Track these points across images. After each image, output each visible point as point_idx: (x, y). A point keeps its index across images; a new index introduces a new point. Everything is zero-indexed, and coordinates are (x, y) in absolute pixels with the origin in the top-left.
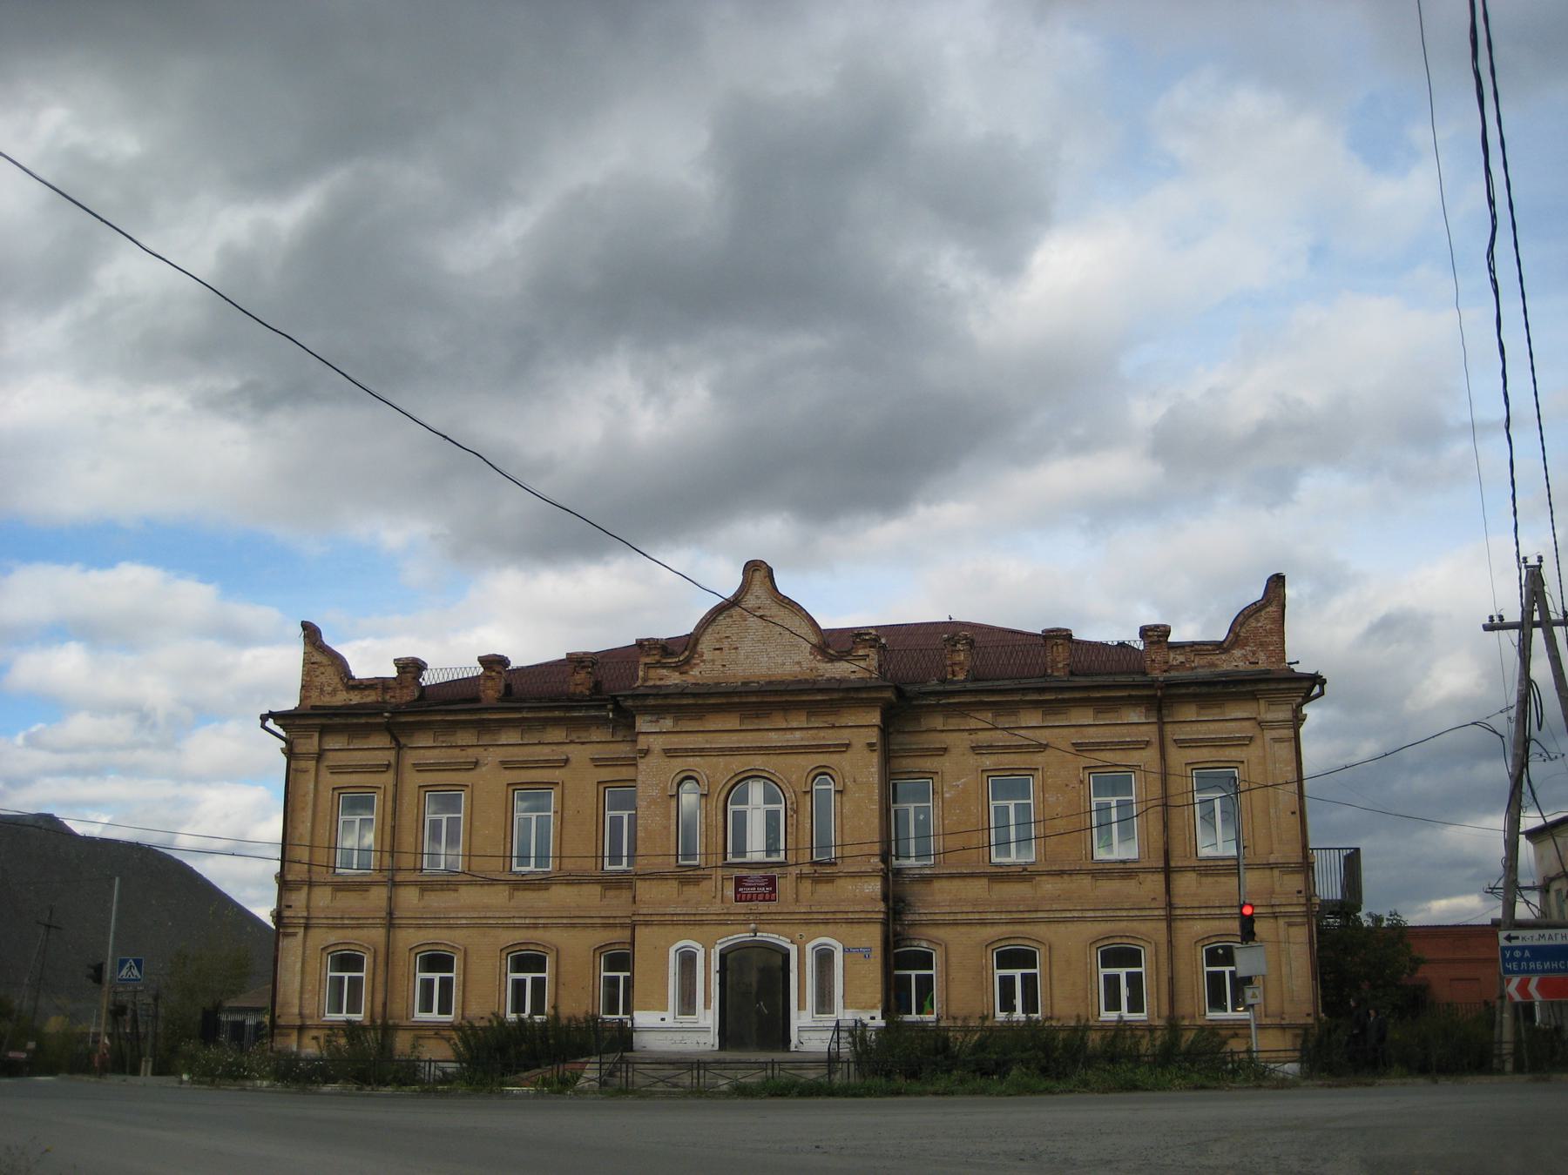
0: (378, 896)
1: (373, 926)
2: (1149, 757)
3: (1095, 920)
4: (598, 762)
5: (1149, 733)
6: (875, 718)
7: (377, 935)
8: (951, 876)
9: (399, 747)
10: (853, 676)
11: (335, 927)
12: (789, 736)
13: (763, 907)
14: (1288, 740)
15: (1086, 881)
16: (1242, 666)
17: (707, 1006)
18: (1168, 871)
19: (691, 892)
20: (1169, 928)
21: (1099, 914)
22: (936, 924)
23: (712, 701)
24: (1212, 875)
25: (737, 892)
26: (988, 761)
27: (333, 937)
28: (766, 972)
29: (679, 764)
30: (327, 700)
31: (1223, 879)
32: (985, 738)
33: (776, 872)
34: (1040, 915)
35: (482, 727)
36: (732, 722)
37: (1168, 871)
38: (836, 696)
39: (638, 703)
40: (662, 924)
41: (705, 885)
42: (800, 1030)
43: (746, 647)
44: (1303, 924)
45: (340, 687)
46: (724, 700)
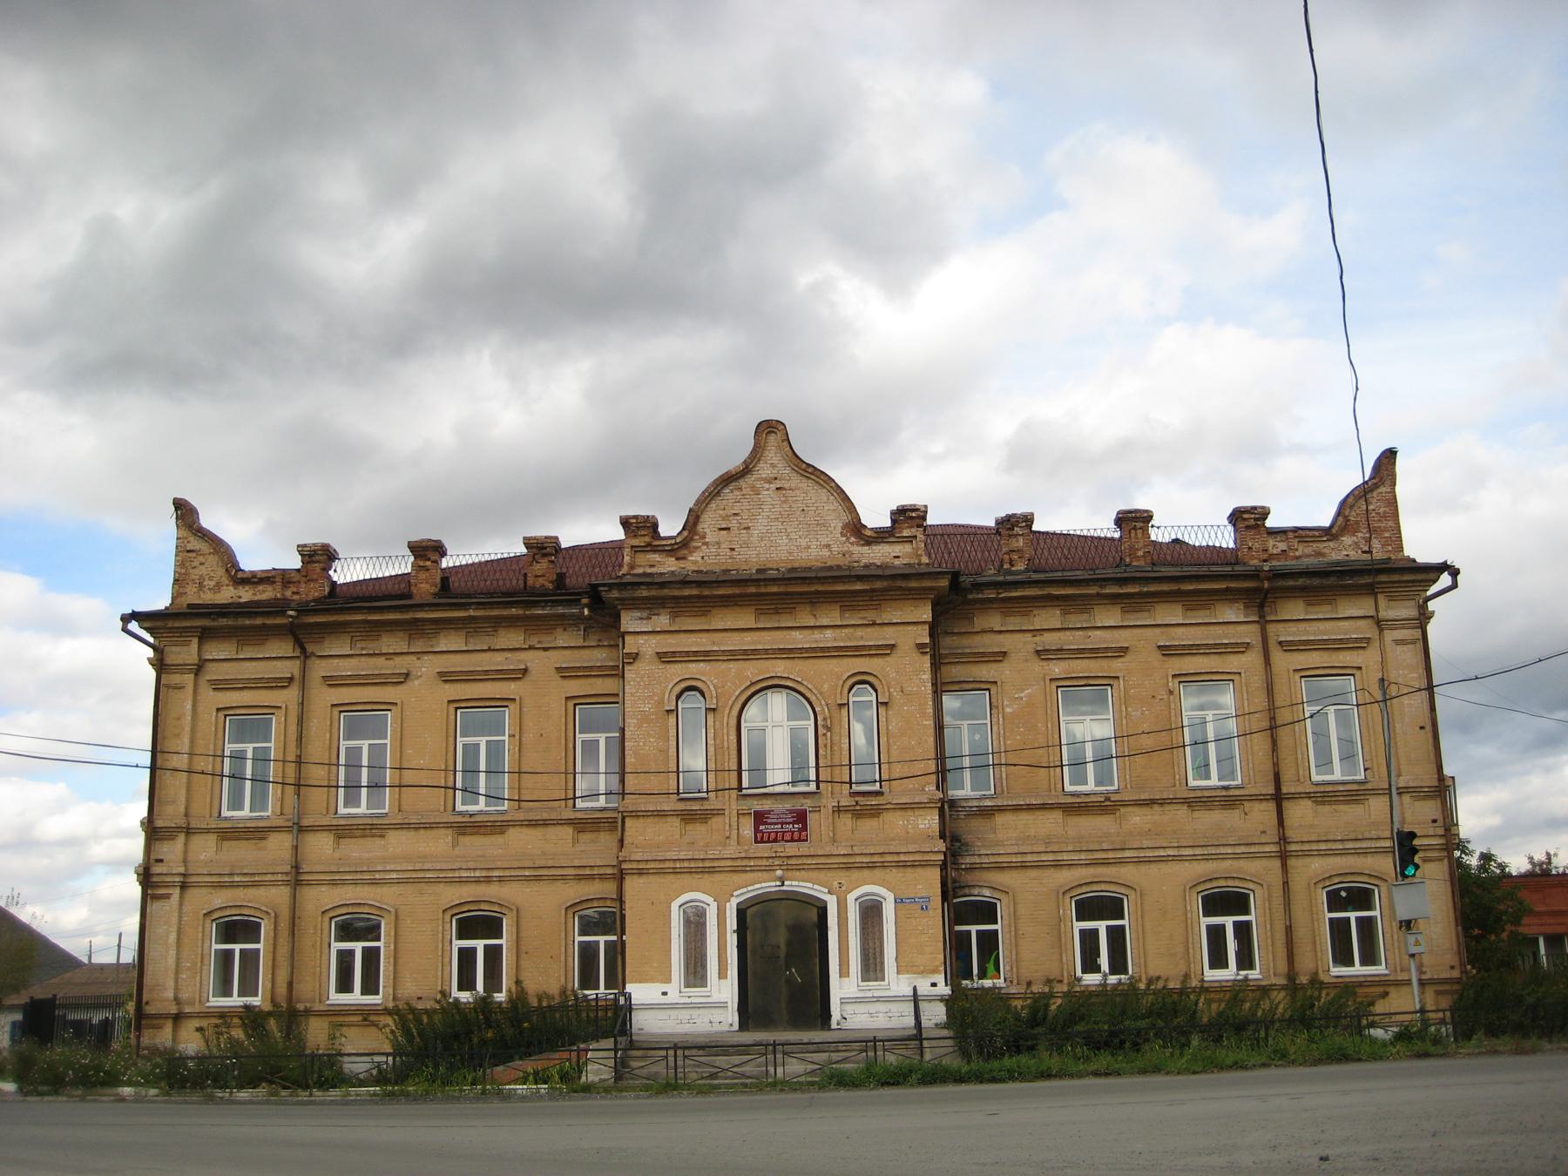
0: (279, 847)
1: (273, 883)
2: (1252, 659)
3: (1194, 858)
4: (565, 673)
5: (1249, 634)
6: (927, 615)
7: (279, 896)
8: (1017, 809)
9: (305, 655)
10: (897, 562)
11: (220, 886)
12: (817, 635)
13: (791, 848)
14: (1413, 642)
15: (1182, 812)
16: (1354, 555)
17: (722, 974)
18: (1279, 798)
19: (698, 831)
20: (1284, 866)
21: (1198, 851)
22: (1000, 868)
23: (721, 592)
24: (1330, 803)
25: (757, 830)
26: (1058, 669)
27: (219, 899)
28: (796, 929)
29: (678, 671)
30: (208, 598)
31: (1342, 807)
32: (1051, 640)
33: (807, 804)
34: (1127, 854)
35: (414, 628)
36: (746, 618)
37: (1279, 798)
38: (878, 585)
39: (626, 594)
40: (660, 872)
41: (716, 822)
42: (843, 1002)
43: (760, 526)
44: (1440, 859)
45: (225, 580)
46: (737, 591)
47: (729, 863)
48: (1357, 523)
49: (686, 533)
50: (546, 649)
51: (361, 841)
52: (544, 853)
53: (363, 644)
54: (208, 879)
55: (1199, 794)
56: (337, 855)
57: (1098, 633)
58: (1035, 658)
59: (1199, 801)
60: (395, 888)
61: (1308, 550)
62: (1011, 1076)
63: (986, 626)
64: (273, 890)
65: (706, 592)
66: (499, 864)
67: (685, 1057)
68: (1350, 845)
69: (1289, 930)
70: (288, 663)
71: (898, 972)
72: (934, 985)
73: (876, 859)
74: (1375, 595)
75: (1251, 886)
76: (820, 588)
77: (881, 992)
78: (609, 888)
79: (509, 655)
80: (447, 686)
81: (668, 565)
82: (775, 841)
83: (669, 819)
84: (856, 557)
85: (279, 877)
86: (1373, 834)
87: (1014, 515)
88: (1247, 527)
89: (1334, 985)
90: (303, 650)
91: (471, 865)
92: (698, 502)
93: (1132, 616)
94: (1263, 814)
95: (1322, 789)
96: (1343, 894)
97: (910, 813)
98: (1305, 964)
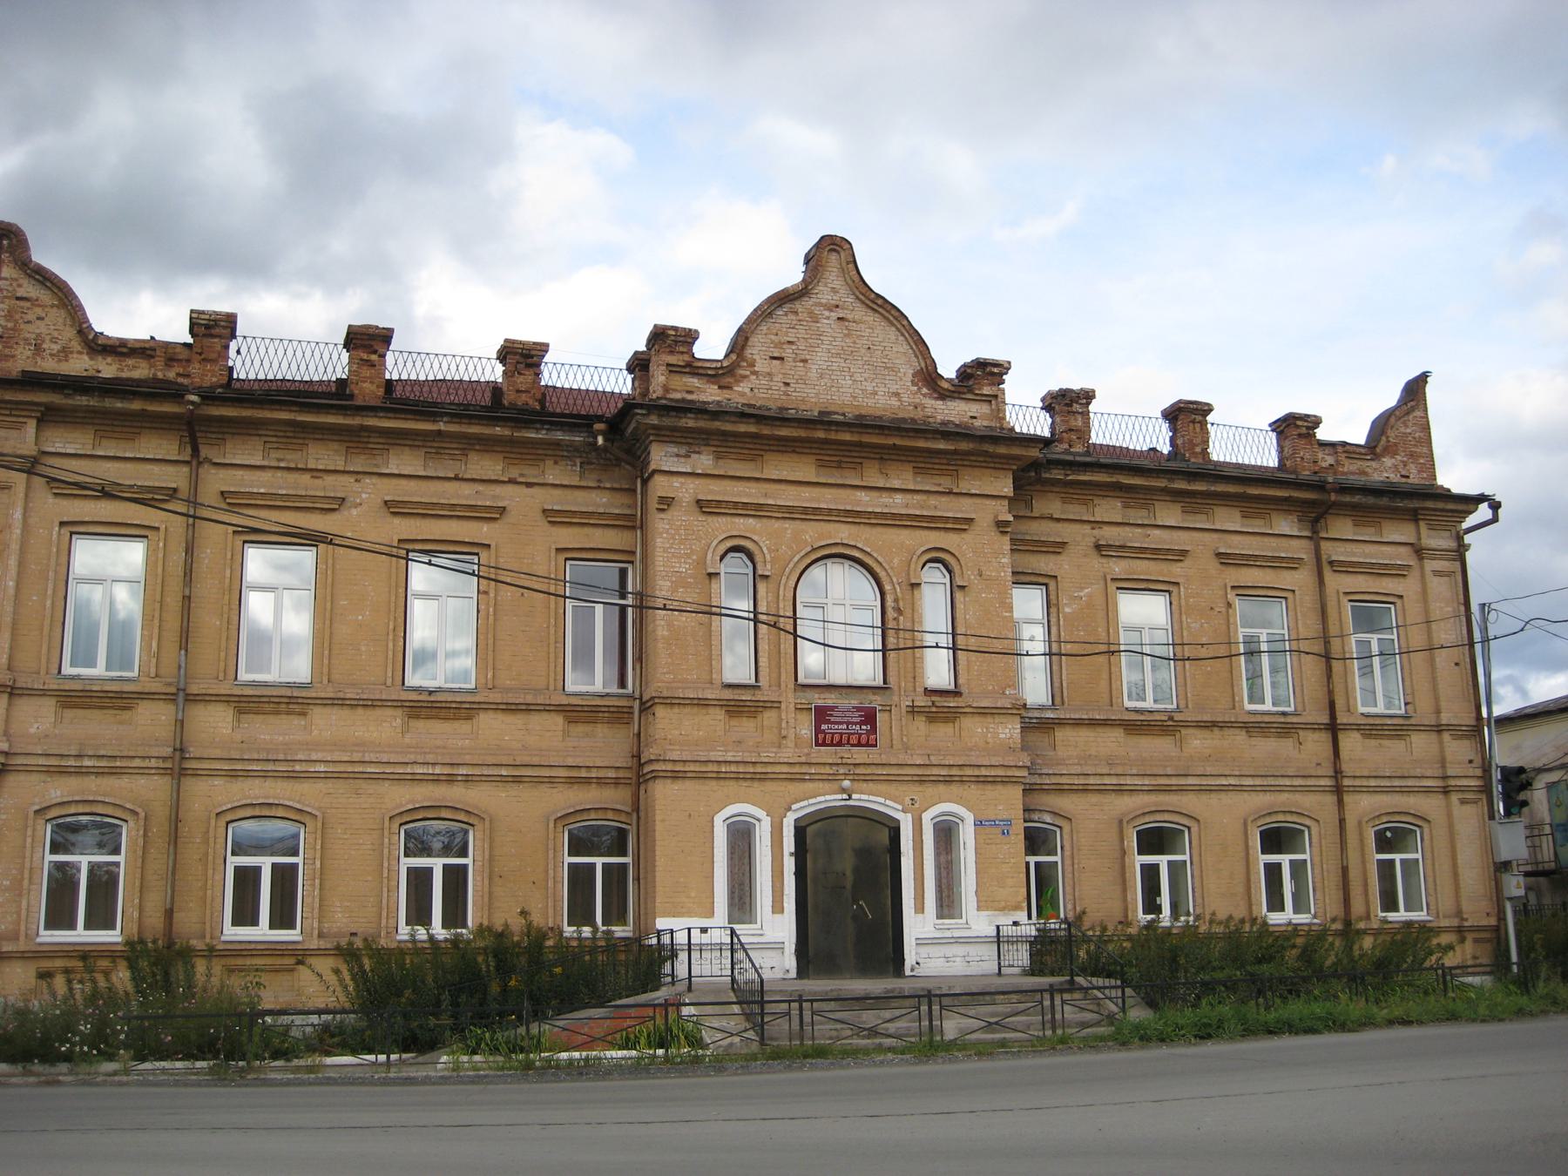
0: (153, 720)
1: (142, 772)
2: (1300, 580)
3: (1253, 789)
4: (553, 517)
5: (1301, 549)
6: (1007, 488)
7: (152, 790)
8: (1078, 723)
9: (196, 460)
10: (977, 423)
11: (63, 772)
12: (886, 499)
13: (860, 754)
14: (1449, 574)
15: (1240, 737)
16: (1395, 478)
17: (778, 908)
18: (1333, 729)
19: (746, 726)
20: (1340, 802)
21: (1258, 782)
22: (1060, 790)
23: (784, 432)
24: (1376, 737)
25: (818, 731)
26: (1118, 568)
27: (57, 790)
28: (865, 854)
29: (723, 527)
30: (48, 365)
31: (1386, 742)
32: (1110, 535)
33: (876, 701)
34: (1191, 781)
35: (354, 439)
36: (805, 469)
37: (1333, 729)
38: (964, 446)
39: (667, 421)
40: (701, 777)
41: (769, 717)
42: (921, 942)
43: (819, 360)
44: (1475, 802)
45: (76, 345)
46: (802, 433)
47: (785, 769)
48: (1396, 445)
49: (734, 357)
50: (529, 485)
51: (271, 719)
52: (525, 748)
53: (279, 454)
54: (42, 761)
55: (1259, 719)
56: (238, 737)
57: (1157, 532)
58: (1093, 553)
59: (1257, 727)
60: (321, 786)
61: (1353, 468)
62: (1291, 1028)
63: (1046, 512)
64: (142, 781)
65: (766, 431)
66: (468, 759)
67: (1063, 1002)
68: (1397, 783)
69: (1345, 870)
70: (171, 469)
71: (979, 909)
72: (1015, 924)
73: (954, 772)
74: (1416, 521)
75: (1307, 822)
76: (898, 442)
77: (955, 934)
78: (616, 798)
79: (480, 487)
80: (397, 521)
81: (710, 394)
82: (840, 744)
83: (712, 710)
84: (929, 412)
85: (153, 763)
86: (1418, 772)
87: (1071, 391)
88: (1300, 435)
89: (1377, 933)
90: (195, 451)
91: (430, 758)
92: (749, 321)
93: (1191, 517)
94: (1316, 744)
95: (1371, 721)
96: (1389, 834)
97: (990, 719)
98: (1357, 907)
